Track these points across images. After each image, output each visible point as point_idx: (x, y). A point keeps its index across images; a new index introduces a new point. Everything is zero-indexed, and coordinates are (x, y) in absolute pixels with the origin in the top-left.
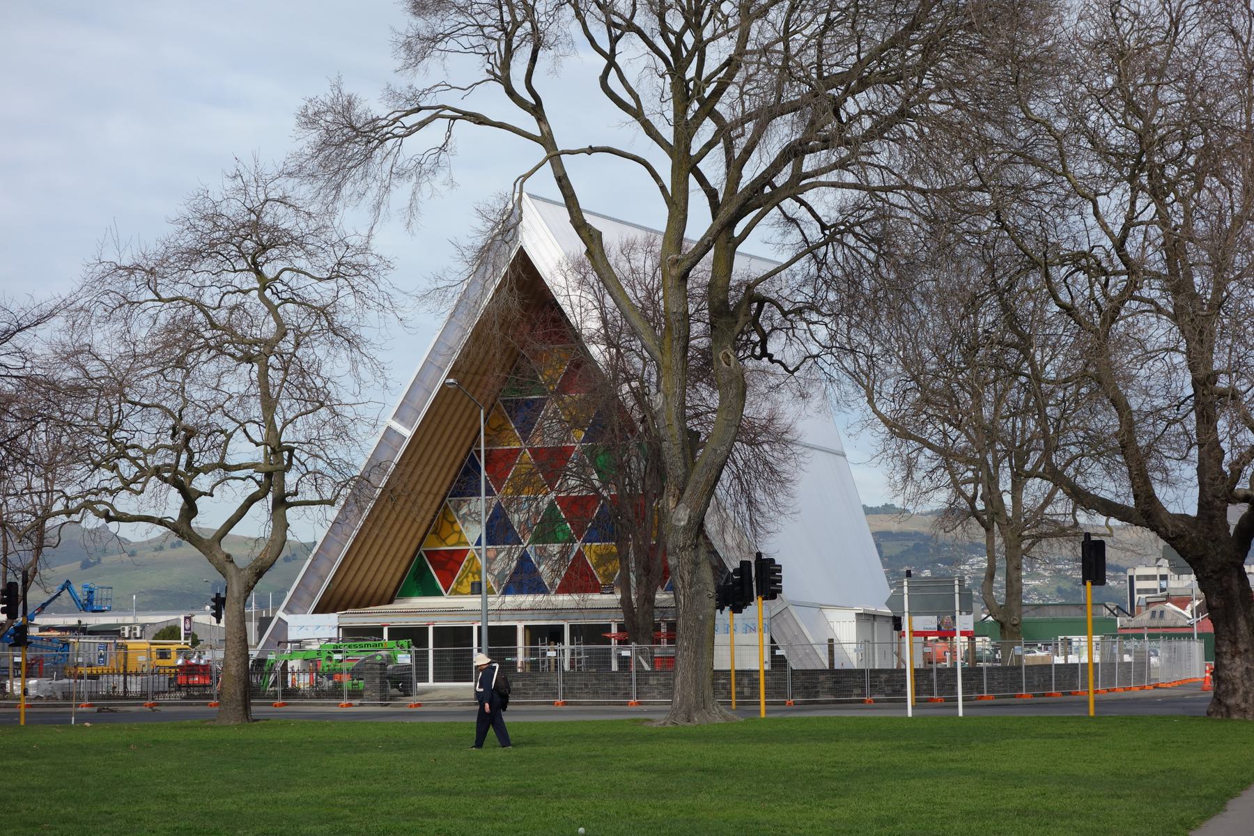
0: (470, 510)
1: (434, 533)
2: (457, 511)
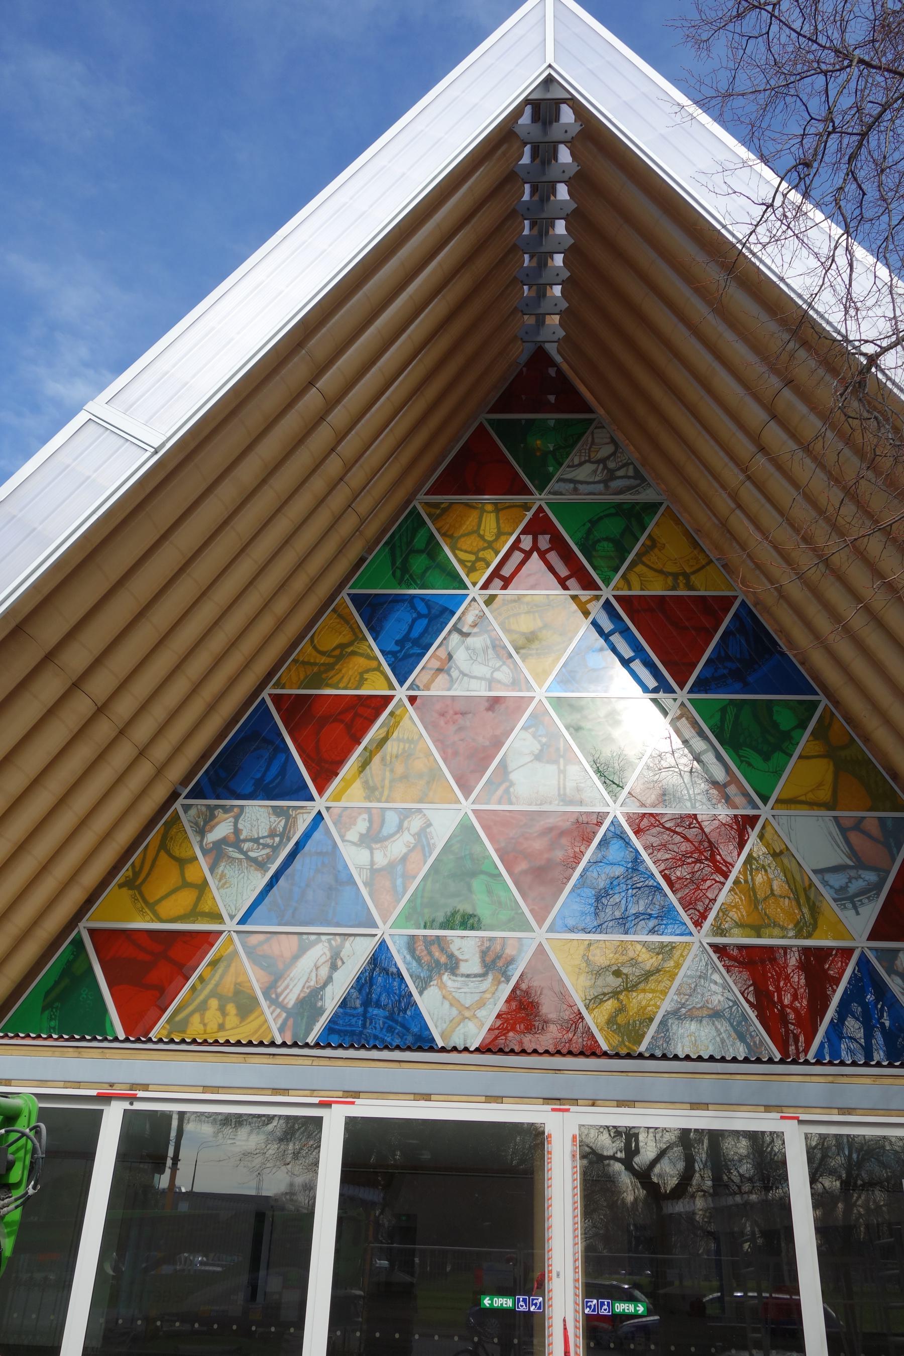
0: (237, 831)
1: (128, 884)
2: (202, 832)
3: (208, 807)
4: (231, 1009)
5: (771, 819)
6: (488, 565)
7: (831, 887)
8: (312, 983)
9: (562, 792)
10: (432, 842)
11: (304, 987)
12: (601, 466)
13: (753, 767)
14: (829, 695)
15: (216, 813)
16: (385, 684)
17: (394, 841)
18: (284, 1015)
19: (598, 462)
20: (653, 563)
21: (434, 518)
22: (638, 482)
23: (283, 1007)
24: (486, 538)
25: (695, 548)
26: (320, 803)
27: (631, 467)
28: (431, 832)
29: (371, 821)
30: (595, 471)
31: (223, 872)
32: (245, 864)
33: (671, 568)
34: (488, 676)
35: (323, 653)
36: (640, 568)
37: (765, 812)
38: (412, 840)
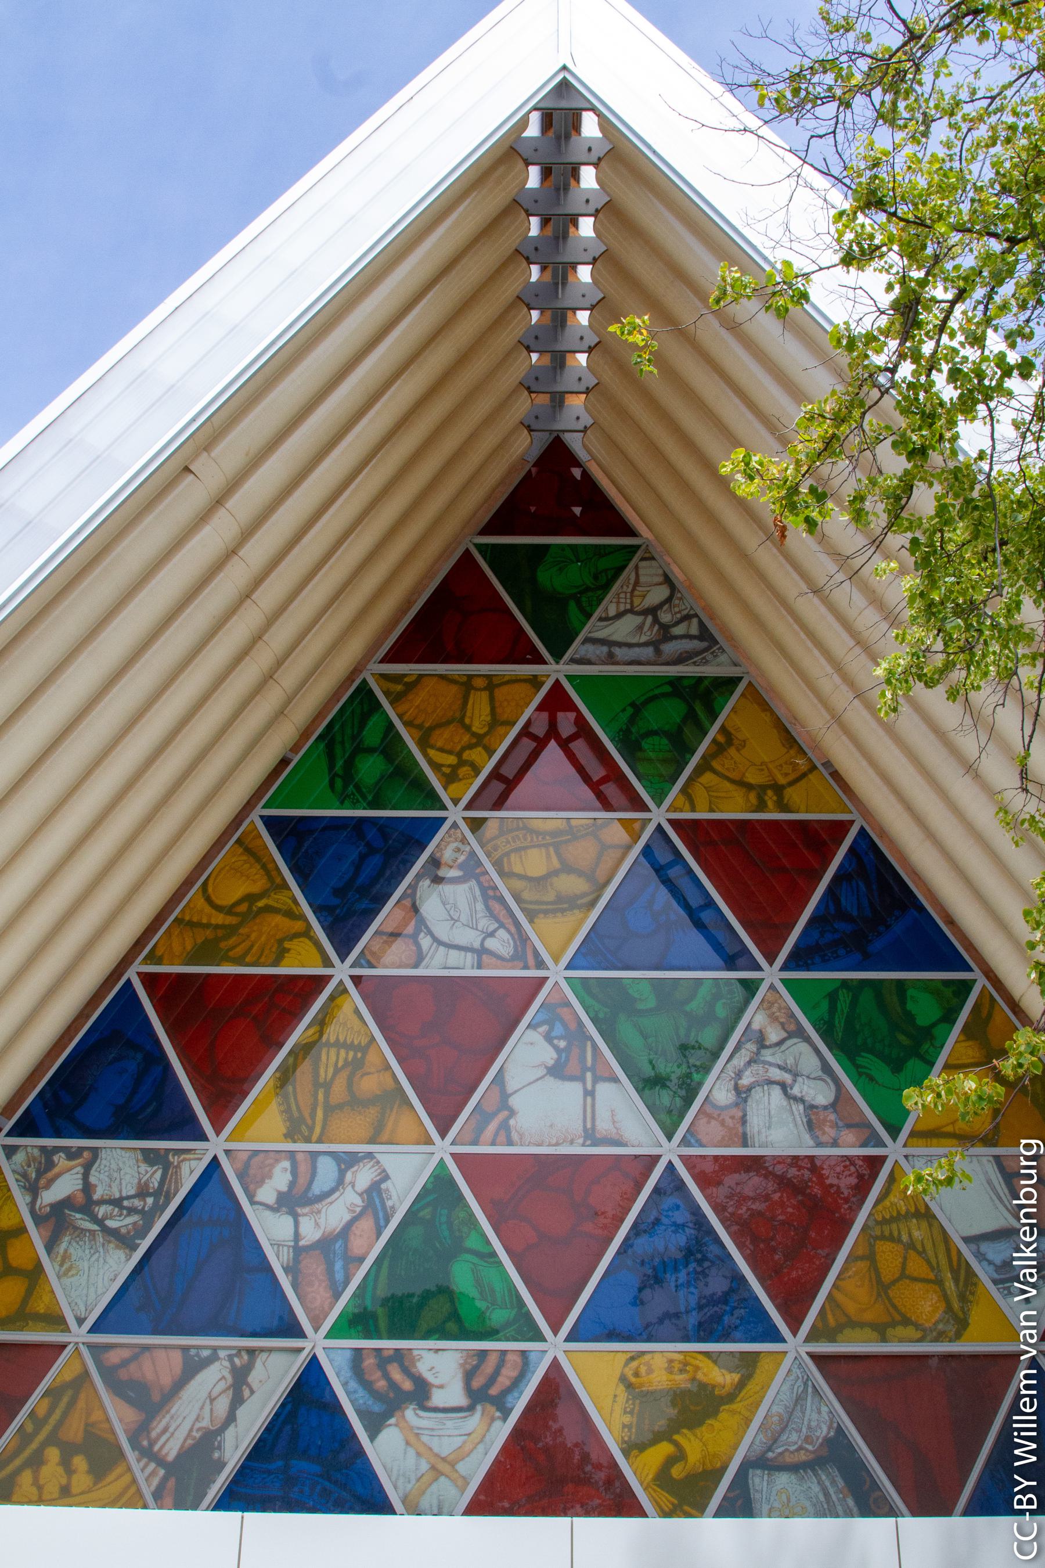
0: (87, 1188)
2: (33, 1189)
3: (43, 1149)
4: (80, 1462)
5: (903, 1162)
6: (477, 772)
7: (990, 1263)
8: (205, 1423)
9: (589, 1125)
10: (389, 1203)
11: (191, 1430)
12: (650, 619)
13: (877, 1082)
14: (990, 974)
15: (56, 1158)
16: (319, 960)
17: (331, 1203)
18: (162, 1472)
19: (645, 612)
20: (728, 769)
21: (395, 699)
22: (705, 644)
23: (161, 1462)
24: (474, 729)
25: (791, 747)
26: (215, 1145)
27: (695, 621)
28: (387, 1190)
29: (294, 1172)
30: (640, 628)
31: (66, 1251)
32: (100, 1239)
33: (752, 778)
34: (477, 945)
35: (218, 908)
36: (708, 778)
37: (893, 1150)
38: (358, 1201)
